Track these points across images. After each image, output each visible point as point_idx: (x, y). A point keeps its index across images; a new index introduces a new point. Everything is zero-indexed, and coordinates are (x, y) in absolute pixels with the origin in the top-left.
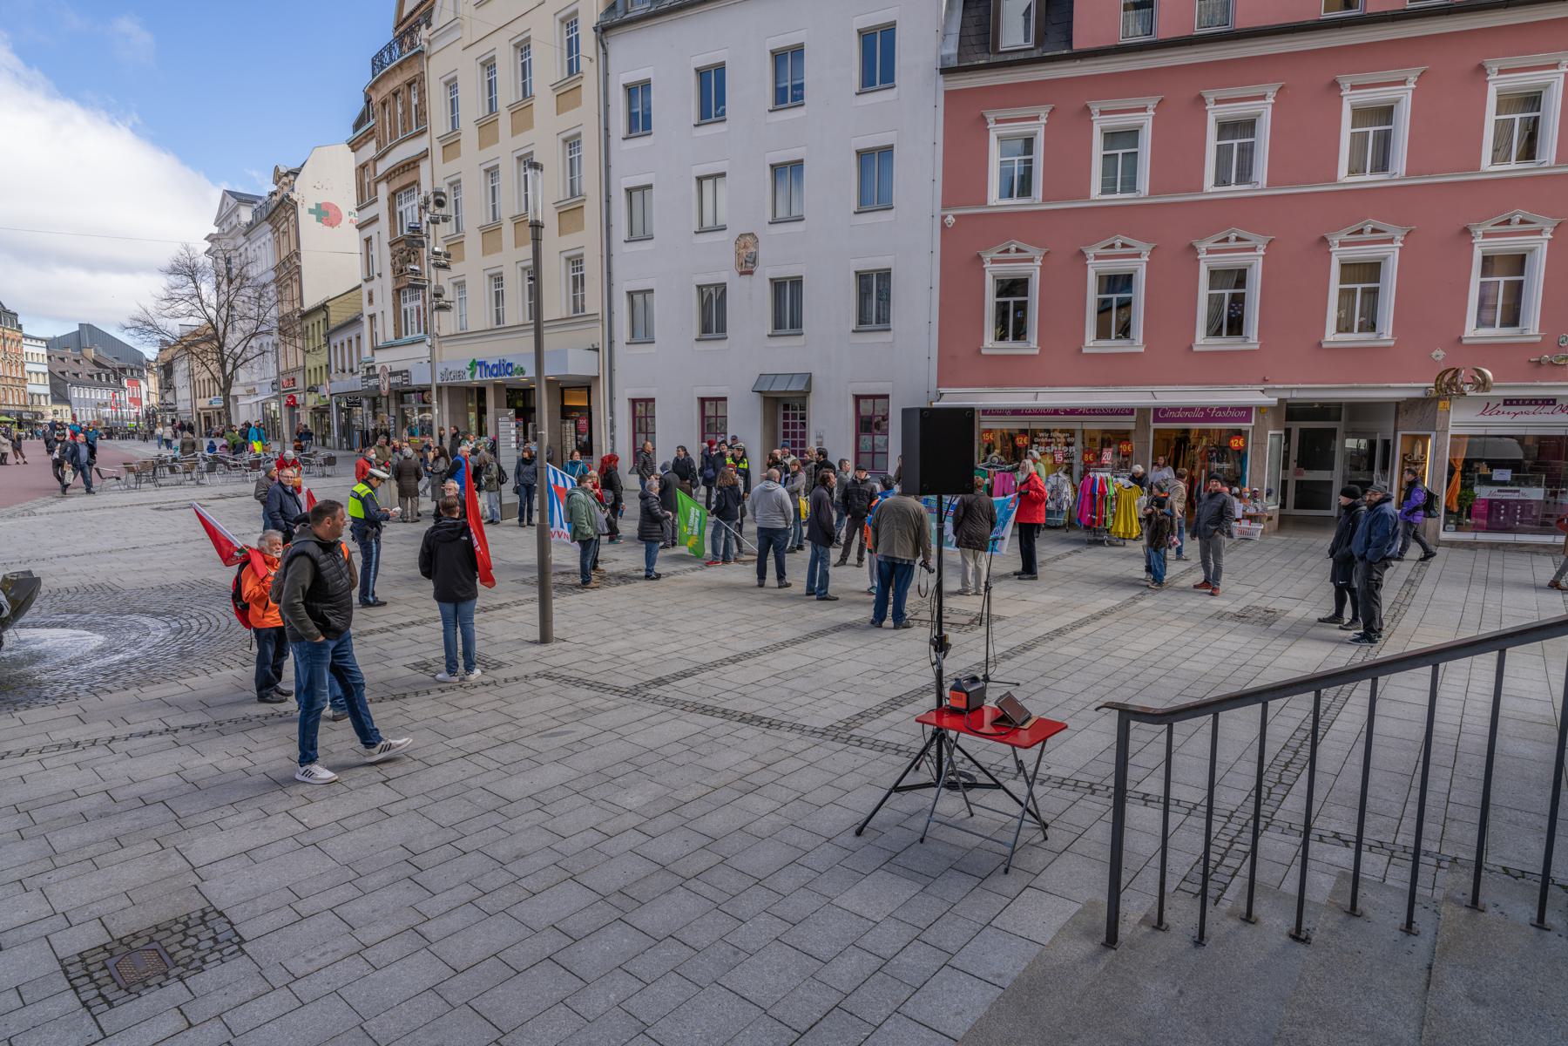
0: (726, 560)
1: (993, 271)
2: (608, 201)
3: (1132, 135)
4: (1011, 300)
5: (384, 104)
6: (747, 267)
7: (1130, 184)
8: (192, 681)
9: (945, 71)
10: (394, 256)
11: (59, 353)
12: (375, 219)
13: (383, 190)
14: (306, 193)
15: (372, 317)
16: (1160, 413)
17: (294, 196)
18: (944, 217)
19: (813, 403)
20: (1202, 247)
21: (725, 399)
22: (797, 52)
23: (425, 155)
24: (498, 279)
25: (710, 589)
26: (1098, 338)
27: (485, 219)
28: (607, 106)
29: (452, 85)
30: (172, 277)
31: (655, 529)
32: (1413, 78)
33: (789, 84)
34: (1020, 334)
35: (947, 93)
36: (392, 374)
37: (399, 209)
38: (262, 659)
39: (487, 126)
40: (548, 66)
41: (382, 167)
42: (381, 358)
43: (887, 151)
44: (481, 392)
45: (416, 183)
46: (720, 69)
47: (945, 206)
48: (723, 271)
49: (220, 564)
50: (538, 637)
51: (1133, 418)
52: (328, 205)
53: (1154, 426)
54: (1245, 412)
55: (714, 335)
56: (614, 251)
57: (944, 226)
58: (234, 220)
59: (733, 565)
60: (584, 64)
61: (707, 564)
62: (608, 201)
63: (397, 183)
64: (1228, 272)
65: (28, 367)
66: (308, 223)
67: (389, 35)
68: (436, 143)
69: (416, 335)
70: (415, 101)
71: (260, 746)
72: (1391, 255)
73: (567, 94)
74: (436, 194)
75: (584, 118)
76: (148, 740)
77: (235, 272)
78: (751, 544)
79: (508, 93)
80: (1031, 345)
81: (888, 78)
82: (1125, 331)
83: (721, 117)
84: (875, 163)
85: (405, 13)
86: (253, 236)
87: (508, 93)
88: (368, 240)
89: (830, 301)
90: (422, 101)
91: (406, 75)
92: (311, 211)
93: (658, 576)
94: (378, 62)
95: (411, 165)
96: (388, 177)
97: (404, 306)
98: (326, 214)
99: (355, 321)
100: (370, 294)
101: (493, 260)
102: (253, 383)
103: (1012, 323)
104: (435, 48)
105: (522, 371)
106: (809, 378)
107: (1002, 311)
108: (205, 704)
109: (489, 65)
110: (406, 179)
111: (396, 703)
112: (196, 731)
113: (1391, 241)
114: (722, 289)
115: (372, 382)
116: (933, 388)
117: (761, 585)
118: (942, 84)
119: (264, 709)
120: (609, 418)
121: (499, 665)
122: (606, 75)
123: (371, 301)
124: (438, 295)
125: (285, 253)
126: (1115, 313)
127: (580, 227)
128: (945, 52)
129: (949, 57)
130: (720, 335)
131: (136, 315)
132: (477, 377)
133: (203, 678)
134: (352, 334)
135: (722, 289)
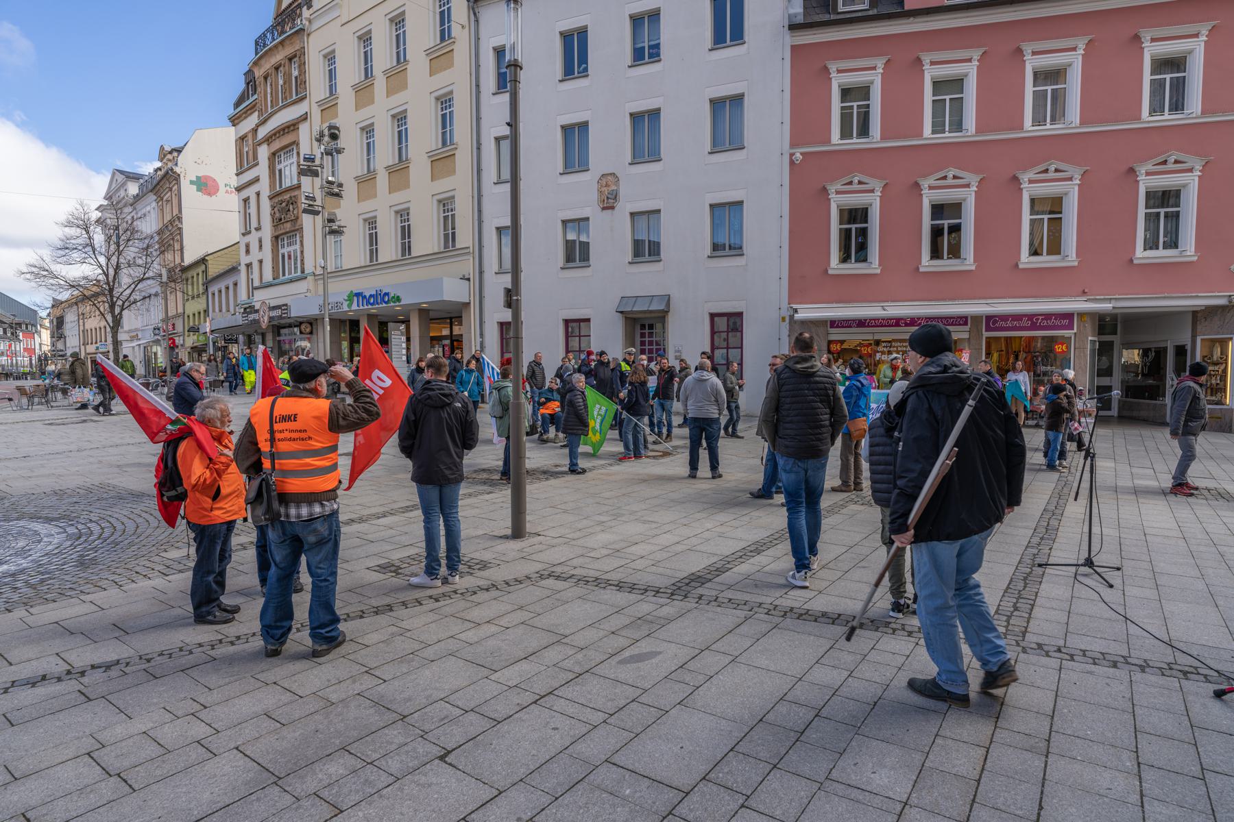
0: (637, 455)
1: (837, 202)
2: (478, 149)
3: (957, 84)
4: (854, 227)
5: (266, 78)
6: (609, 202)
7: (958, 125)
8: (98, 597)
9: (793, 27)
10: (273, 207)
12: (257, 180)
13: (264, 152)
14: (188, 168)
15: (249, 266)
16: (992, 321)
17: (177, 170)
18: (792, 155)
19: (672, 322)
20: (1025, 177)
21: (588, 320)
22: (654, 16)
23: (304, 118)
24: (371, 223)
25: (645, 481)
26: (932, 258)
27: (360, 170)
28: (478, 66)
29: (330, 58)
30: (67, 229)
31: (573, 423)
32: (1205, 32)
33: (646, 45)
34: (863, 258)
35: (794, 48)
36: (274, 308)
37: (278, 167)
38: (201, 569)
39: (363, 91)
40: (421, 33)
41: (262, 132)
42: (260, 296)
43: (737, 100)
44: (354, 324)
45: (296, 143)
46: (583, 33)
47: (793, 145)
48: (588, 207)
49: (144, 437)
50: (509, 532)
51: (967, 328)
52: (207, 178)
53: (986, 334)
54: (1067, 318)
55: (578, 263)
56: (485, 192)
57: (792, 163)
58: (122, 193)
59: (644, 460)
60: (456, 31)
61: (620, 460)
62: (478, 149)
63: (277, 145)
64: (1043, 200)
66: (189, 192)
67: (269, 21)
68: (315, 106)
69: (293, 275)
70: (295, 73)
71: (215, 696)
72: (1191, 184)
73: (440, 58)
74: (330, 128)
75: (457, 78)
76: (41, 691)
78: (682, 435)
79: (383, 58)
80: (874, 265)
81: (738, 36)
82: (955, 252)
83: (584, 73)
84: (727, 111)
85: (284, 7)
86: (139, 206)
87: (383, 58)
88: (246, 200)
89: (685, 233)
90: (302, 72)
91: (289, 51)
92: (192, 182)
93: (584, 471)
94: (259, 42)
95: (292, 127)
96: (268, 140)
97: (281, 251)
98: (206, 186)
99: (233, 270)
100: (247, 246)
101: (368, 206)
102: (137, 330)
103: (855, 245)
104: (315, 26)
105: (398, 299)
106: (668, 299)
107: (846, 236)
108: (121, 629)
109: (365, 39)
110: (286, 140)
111: (383, 619)
112: (114, 672)
113: (1191, 170)
115: (252, 317)
116: (785, 305)
117: (693, 476)
118: (789, 39)
119: (205, 634)
120: (479, 340)
121: (484, 565)
122: (478, 39)
123: (248, 252)
124: (330, 221)
125: (168, 218)
126: (945, 239)
127: (452, 172)
128: (792, 11)
129: (796, 15)
131: (33, 261)
132: (354, 307)
133: (113, 592)
134: (229, 281)
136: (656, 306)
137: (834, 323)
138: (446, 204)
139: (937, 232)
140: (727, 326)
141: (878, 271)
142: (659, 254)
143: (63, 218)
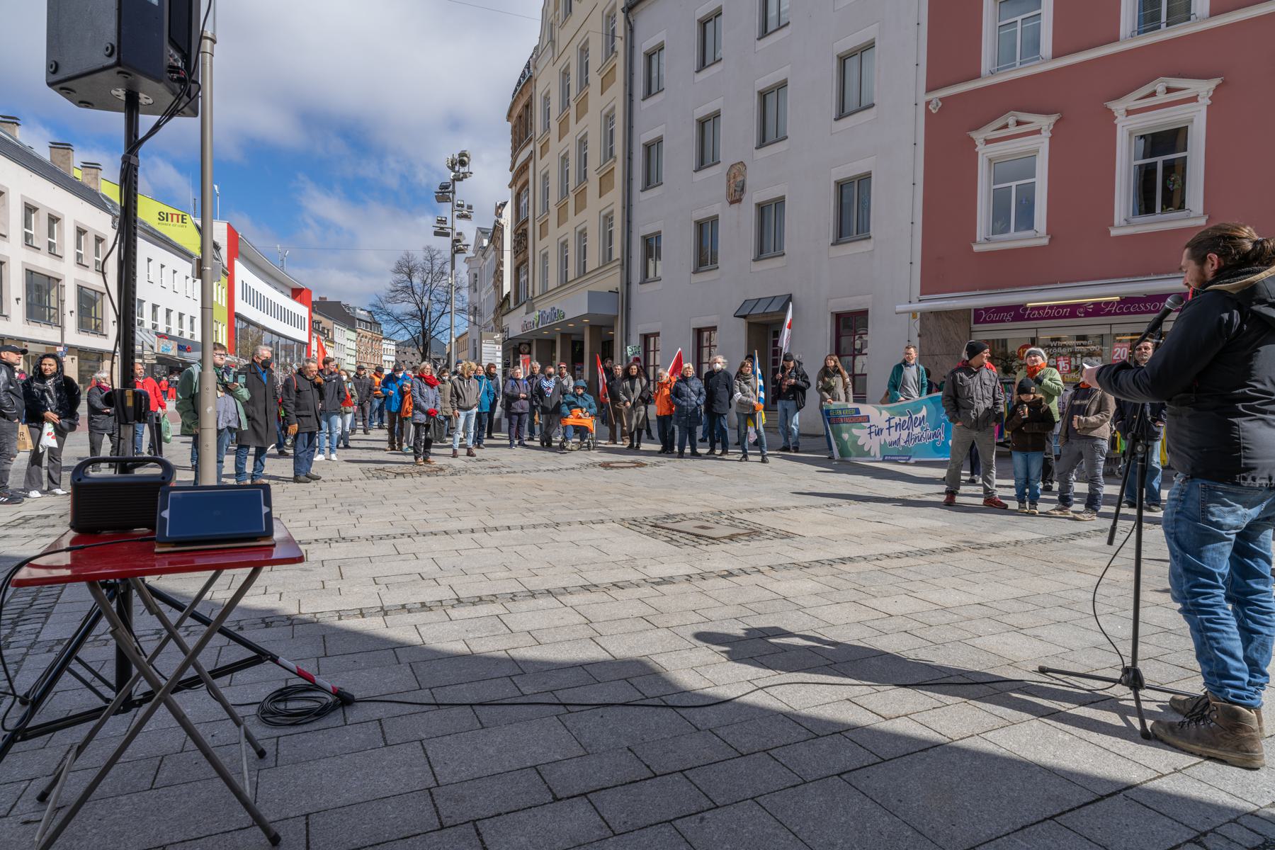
11: (402, 348)
18: (928, 103)
23: (531, 156)
29: (546, 99)
47: (929, 89)
48: (716, 206)
57: (928, 112)
62: (630, 158)
65: (384, 358)
77: (436, 269)
89: (810, 217)
114: (714, 220)
122: (632, 47)
124: (458, 241)
130: (714, 266)
135: (714, 220)
136: (774, 308)
137: (981, 315)
138: (608, 219)
139: (1146, 177)
140: (849, 325)
141: (1045, 241)
142: (781, 247)
143: (393, 266)
